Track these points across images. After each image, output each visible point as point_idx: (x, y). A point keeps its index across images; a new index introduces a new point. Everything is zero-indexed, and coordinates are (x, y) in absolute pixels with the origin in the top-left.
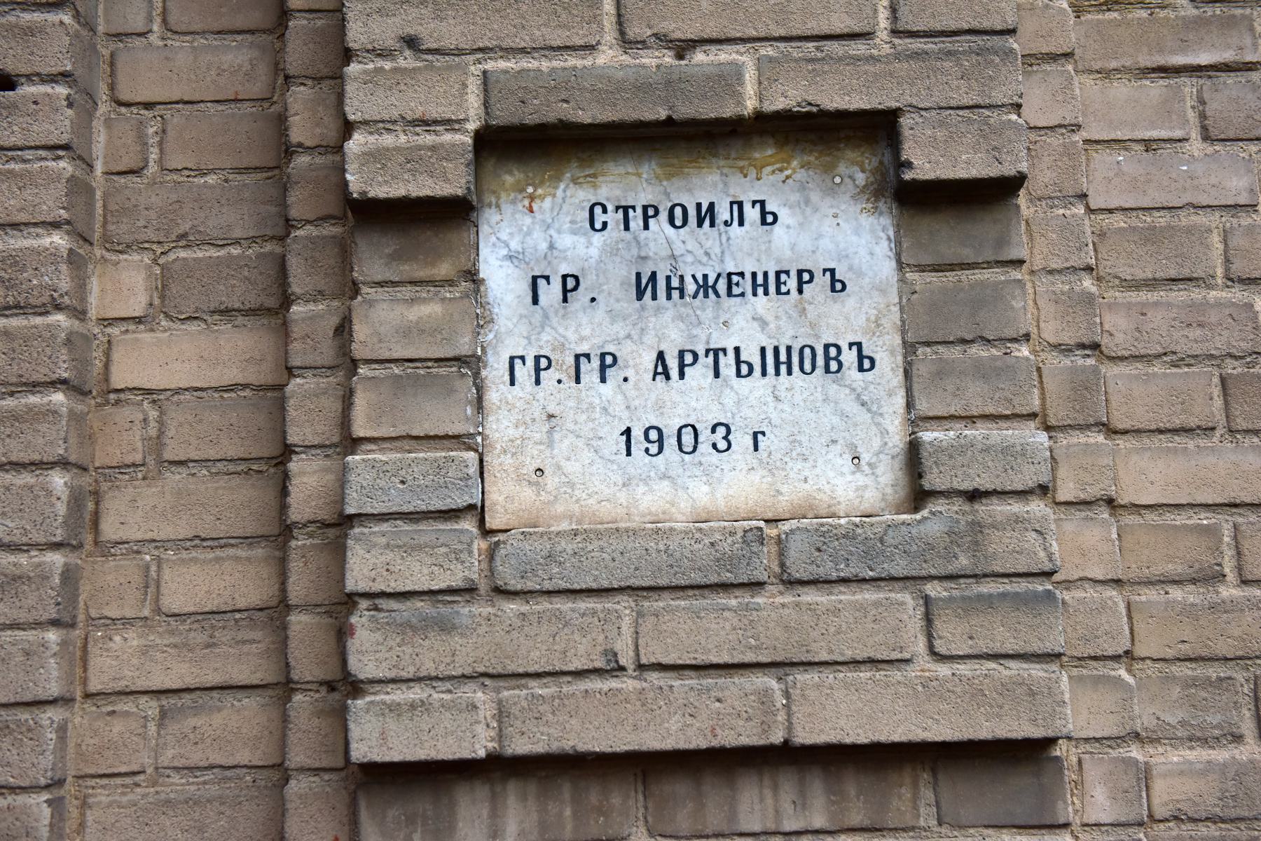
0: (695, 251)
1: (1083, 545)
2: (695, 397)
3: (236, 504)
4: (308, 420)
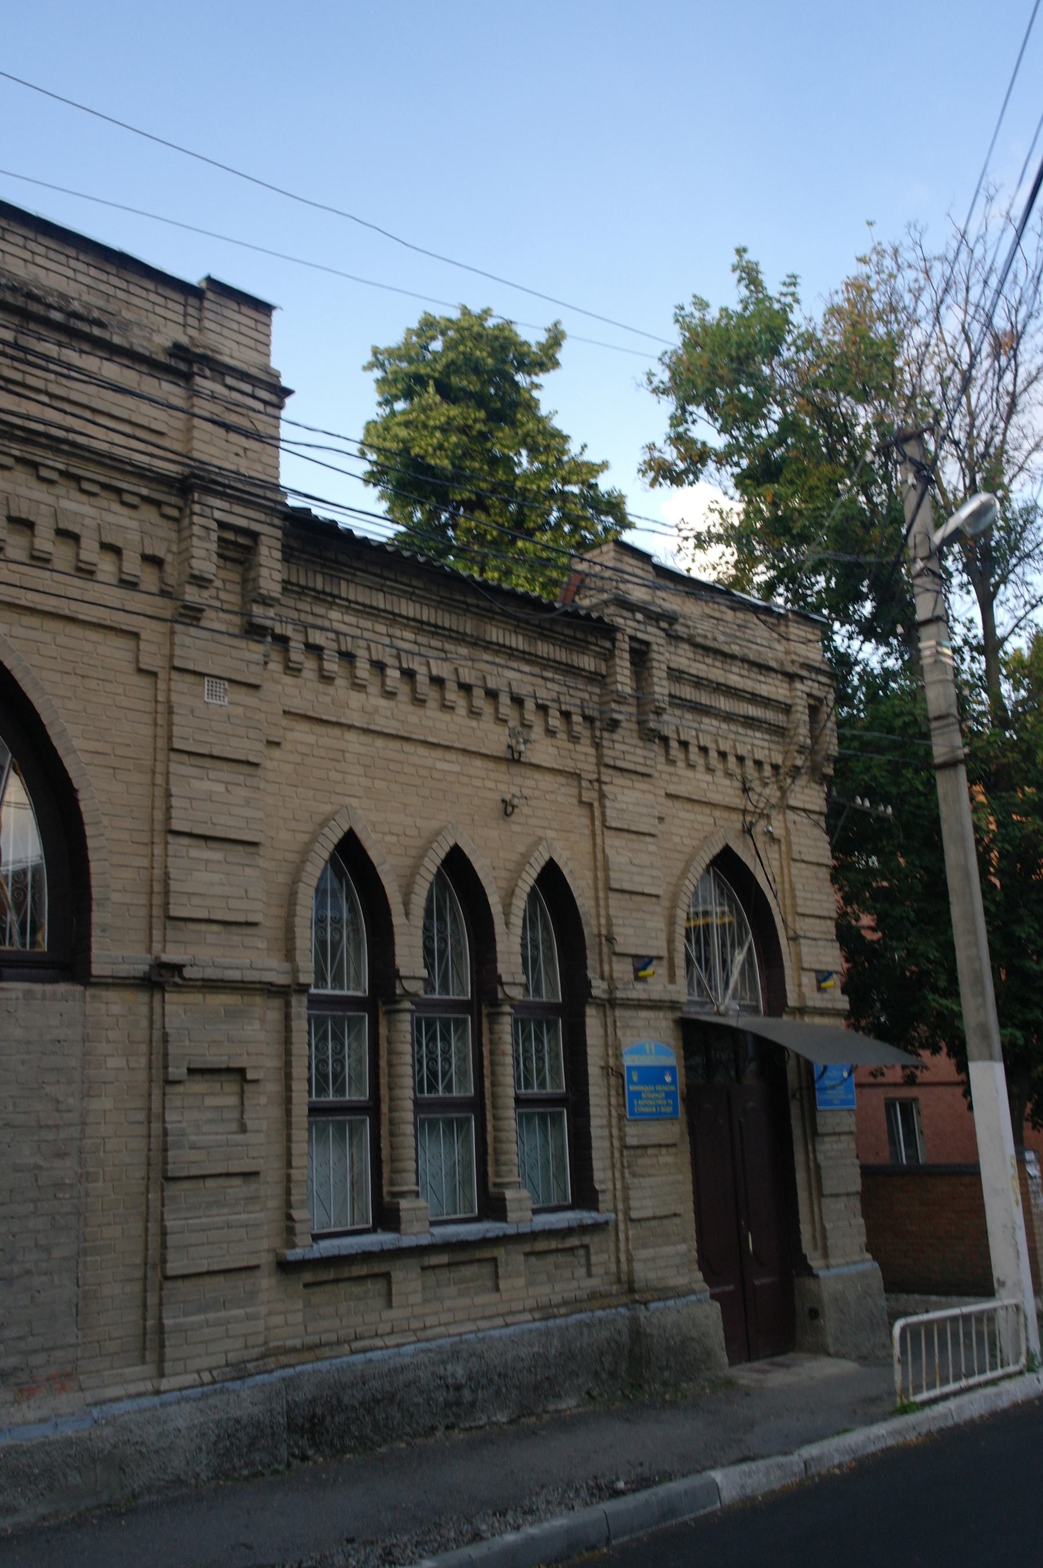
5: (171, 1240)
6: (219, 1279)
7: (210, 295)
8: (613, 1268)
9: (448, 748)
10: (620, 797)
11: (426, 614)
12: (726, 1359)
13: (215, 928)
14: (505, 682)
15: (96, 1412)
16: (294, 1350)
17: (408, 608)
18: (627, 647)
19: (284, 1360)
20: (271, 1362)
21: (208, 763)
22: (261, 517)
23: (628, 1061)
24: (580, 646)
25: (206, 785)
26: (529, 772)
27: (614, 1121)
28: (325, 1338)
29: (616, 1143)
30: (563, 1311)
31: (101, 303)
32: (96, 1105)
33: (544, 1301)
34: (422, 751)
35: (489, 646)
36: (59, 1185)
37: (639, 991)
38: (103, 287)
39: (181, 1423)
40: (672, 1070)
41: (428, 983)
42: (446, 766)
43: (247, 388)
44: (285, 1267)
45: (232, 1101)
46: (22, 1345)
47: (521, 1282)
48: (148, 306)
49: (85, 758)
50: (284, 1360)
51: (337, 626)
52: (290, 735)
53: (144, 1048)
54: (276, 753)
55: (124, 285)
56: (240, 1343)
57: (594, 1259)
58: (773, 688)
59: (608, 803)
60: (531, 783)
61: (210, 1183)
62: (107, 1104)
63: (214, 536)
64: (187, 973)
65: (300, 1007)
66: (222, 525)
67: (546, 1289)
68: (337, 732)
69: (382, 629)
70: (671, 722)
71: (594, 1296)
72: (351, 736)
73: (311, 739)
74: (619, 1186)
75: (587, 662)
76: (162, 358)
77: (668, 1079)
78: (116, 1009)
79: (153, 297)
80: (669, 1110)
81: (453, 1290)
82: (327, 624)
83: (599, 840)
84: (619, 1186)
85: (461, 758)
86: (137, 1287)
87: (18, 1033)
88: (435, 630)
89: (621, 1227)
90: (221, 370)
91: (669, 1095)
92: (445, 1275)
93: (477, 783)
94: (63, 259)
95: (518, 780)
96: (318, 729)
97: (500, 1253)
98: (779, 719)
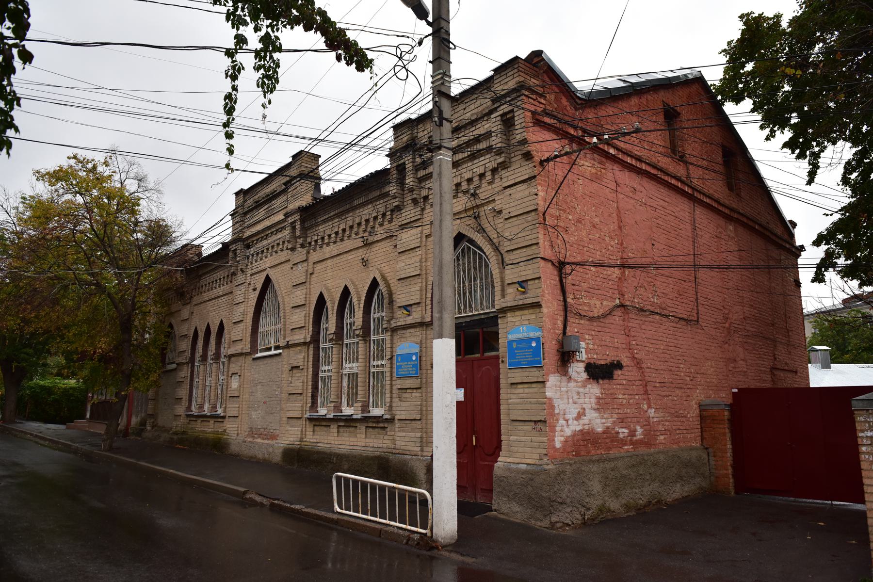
6: (295, 420)
9: (351, 250)
32: (284, 376)
72: (329, 261)
77: (414, 358)
81: (346, 435)
91: (414, 366)
92: (346, 429)
97: (358, 425)
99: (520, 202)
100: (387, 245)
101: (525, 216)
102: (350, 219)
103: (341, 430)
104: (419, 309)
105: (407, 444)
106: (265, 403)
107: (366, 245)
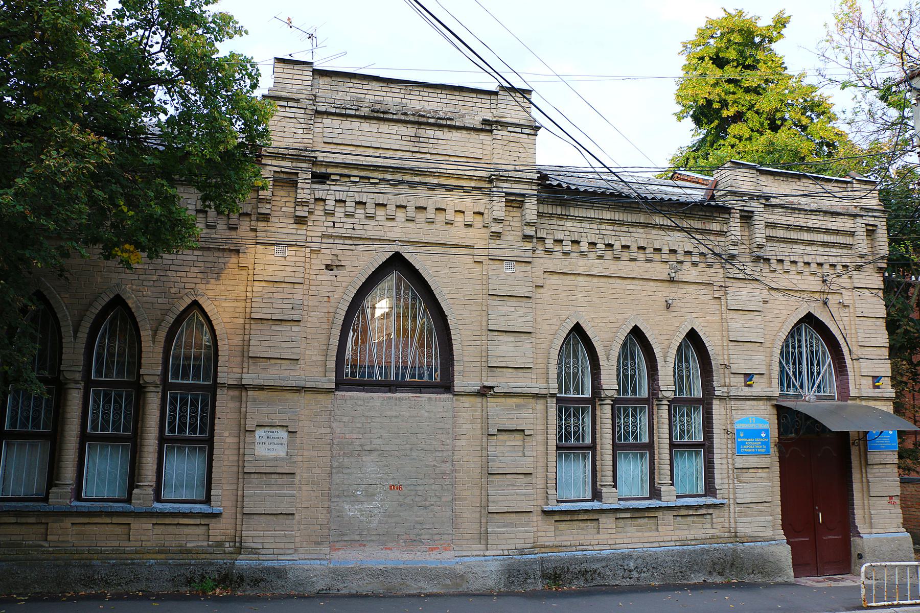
0: (272, 435)
1: (300, 459)
2: (271, 446)
3: (236, 452)
4: (241, 446)
5: (490, 498)
6: (514, 515)
7: (501, 93)
8: (727, 525)
10: (737, 293)
11: (617, 216)
12: (792, 573)
13: (510, 370)
14: (665, 243)
15: (458, 559)
16: (547, 547)
17: (607, 215)
18: (738, 216)
19: (543, 550)
20: (537, 550)
21: (506, 299)
22: (527, 187)
23: (738, 426)
24: (712, 219)
25: (506, 308)
26: (680, 285)
27: (730, 456)
28: (564, 543)
29: (730, 466)
30: (693, 543)
31: (451, 110)
32: (458, 443)
33: (684, 537)
34: (619, 281)
35: (655, 226)
36: (444, 473)
37: (746, 392)
38: (453, 102)
39: (493, 568)
40: (766, 430)
41: (618, 391)
42: (633, 287)
43: (519, 130)
44: (546, 513)
45: (520, 443)
46: (430, 532)
47: (671, 528)
48: (474, 104)
49: (452, 302)
50: (543, 550)
51: (569, 229)
52: (548, 282)
53: (479, 421)
54: (541, 290)
55: (462, 98)
56: (522, 541)
57: (715, 520)
58: (844, 224)
59: (729, 297)
60: (684, 291)
61: (508, 476)
62: (463, 442)
63: (504, 199)
64: (496, 390)
65: (552, 403)
66: (507, 193)
67: (686, 532)
68: (572, 277)
69: (595, 227)
70: (772, 250)
71: (713, 537)
72: (580, 278)
73: (560, 282)
74: (731, 487)
75: (715, 227)
76: (479, 126)
78: (466, 405)
79: (475, 100)
80: (763, 450)
81: (633, 529)
82: (565, 228)
83: (724, 316)
84: (731, 487)
85: (641, 282)
86: (478, 515)
87: (426, 414)
88: (624, 223)
89: (732, 506)
90: (504, 125)
91: (763, 443)
92: (630, 522)
93: (650, 293)
94: (435, 95)
95: (675, 290)
96: (562, 277)
97: (659, 514)
98: (849, 240)
99: (872, 306)
100: (704, 294)
101: (874, 320)
102: (638, 237)
103: (621, 523)
104: (762, 380)
105: (754, 529)
106: (400, 488)
107: (672, 281)
